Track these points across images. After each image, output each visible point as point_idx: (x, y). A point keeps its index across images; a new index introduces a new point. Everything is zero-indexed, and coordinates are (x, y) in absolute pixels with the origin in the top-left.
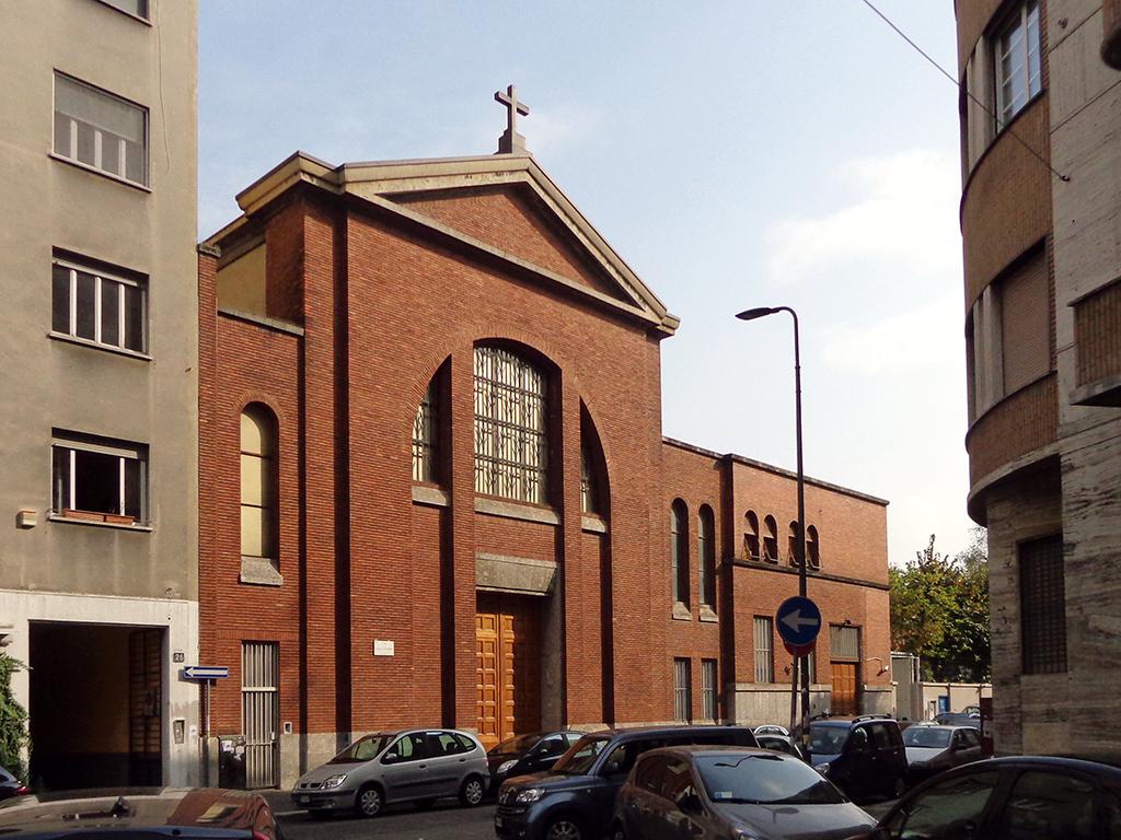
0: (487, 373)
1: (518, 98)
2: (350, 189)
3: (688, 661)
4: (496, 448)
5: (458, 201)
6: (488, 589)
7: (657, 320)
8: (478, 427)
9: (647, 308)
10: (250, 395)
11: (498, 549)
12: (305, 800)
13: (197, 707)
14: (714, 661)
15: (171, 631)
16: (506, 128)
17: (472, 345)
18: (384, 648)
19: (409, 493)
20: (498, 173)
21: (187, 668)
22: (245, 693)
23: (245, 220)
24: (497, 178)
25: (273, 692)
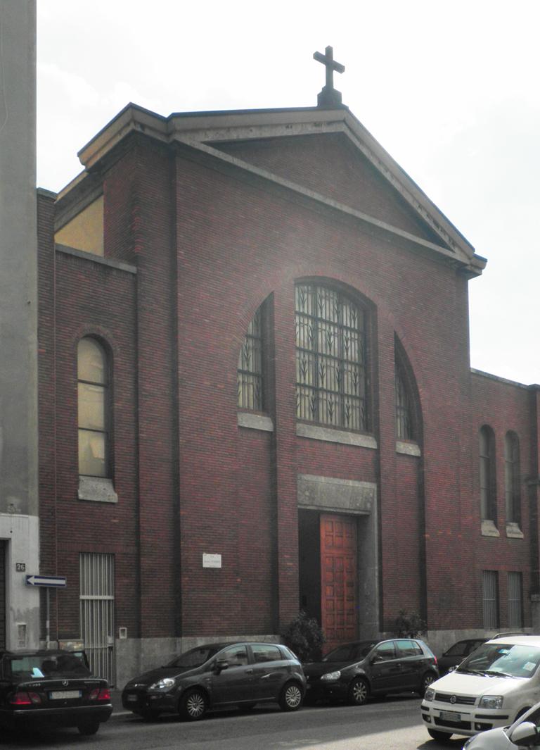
0: (308, 309)
1: (337, 58)
2: (178, 137)
3: (496, 573)
4: (316, 375)
5: (404, 345)
6: (308, 508)
7: (466, 261)
8: (299, 358)
9: (456, 250)
10: (88, 327)
11: (320, 471)
12: (132, 698)
13: (38, 614)
14: (520, 574)
15: (12, 540)
16: (324, 84)
17: (293, 283)
18: (212, 561)
19: (235, 419)
20: (317, 124)
21: (29, 577)
22: (83, 600)
23: (86, 174)
24: (314, 128)
25: (109, 601)
